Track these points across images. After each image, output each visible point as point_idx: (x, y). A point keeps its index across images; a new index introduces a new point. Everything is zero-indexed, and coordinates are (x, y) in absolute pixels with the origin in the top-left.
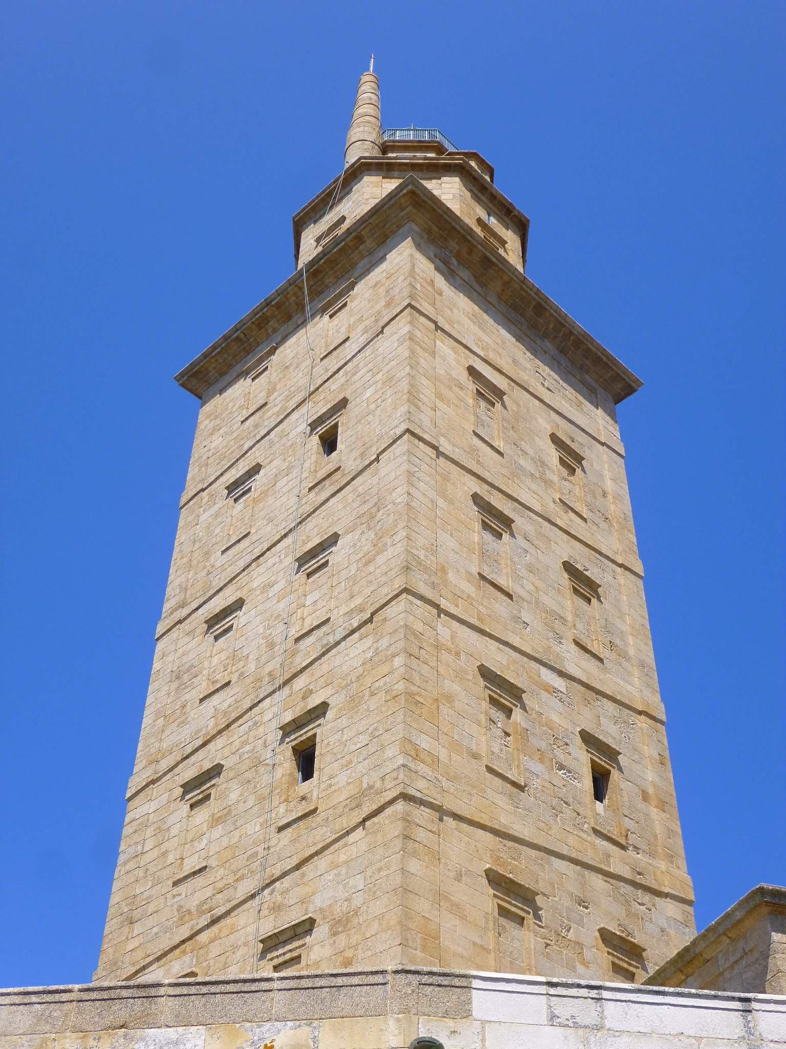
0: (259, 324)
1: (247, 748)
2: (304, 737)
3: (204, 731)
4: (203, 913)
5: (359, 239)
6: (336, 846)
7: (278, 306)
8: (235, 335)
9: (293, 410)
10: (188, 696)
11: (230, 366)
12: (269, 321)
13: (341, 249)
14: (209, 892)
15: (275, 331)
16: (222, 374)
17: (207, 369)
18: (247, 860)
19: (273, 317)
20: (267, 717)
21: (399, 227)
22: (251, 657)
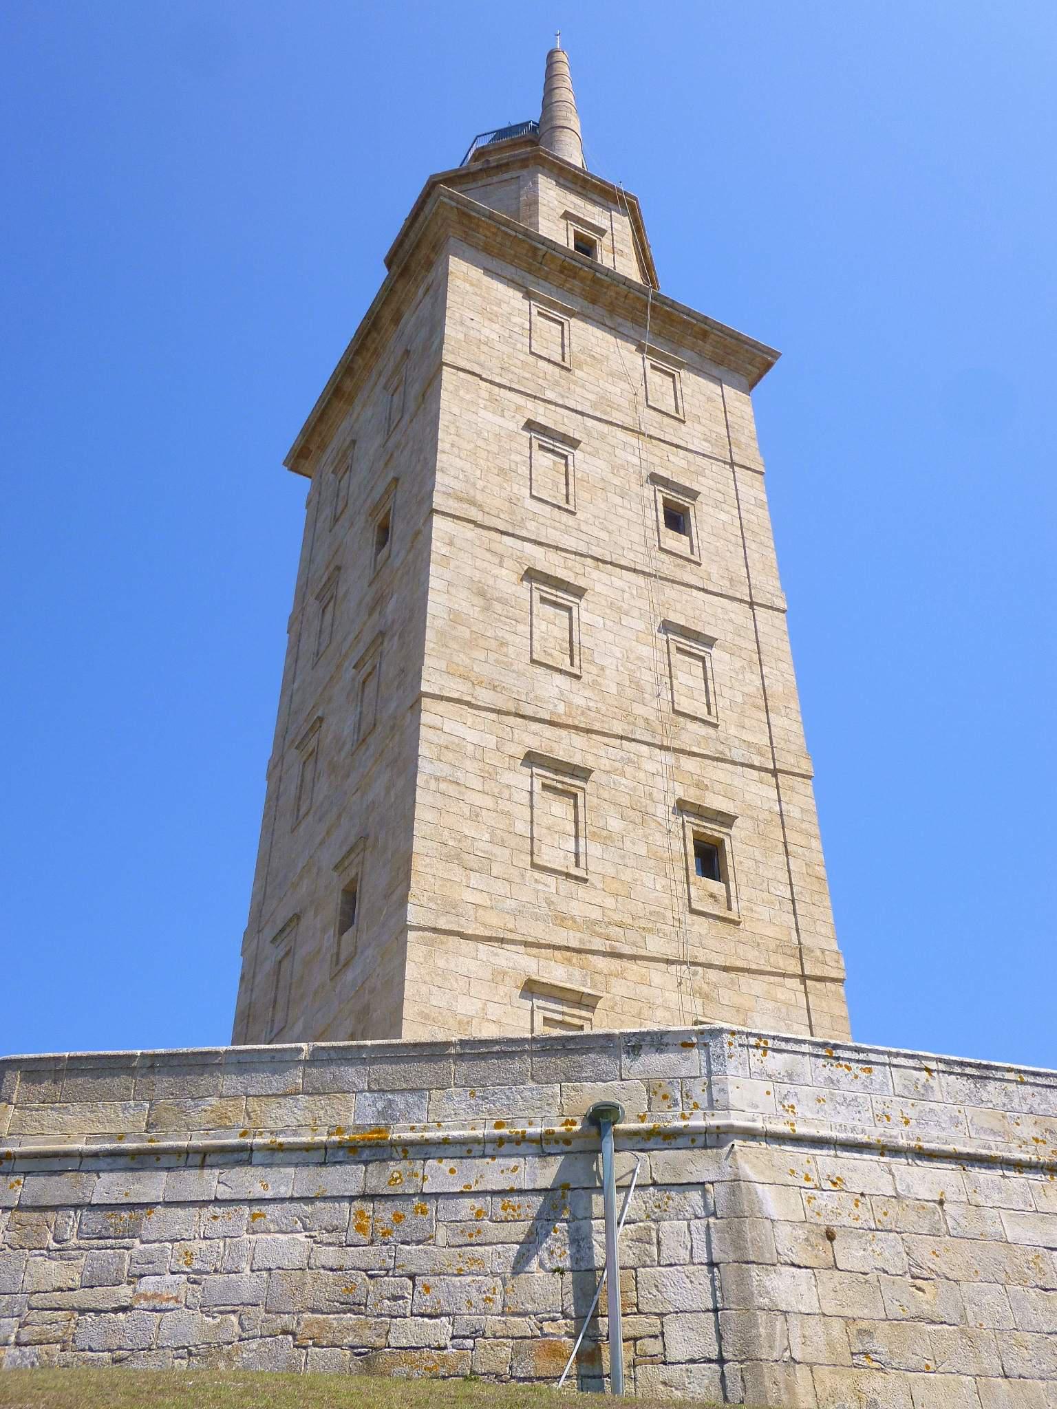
0: (565, 268)
1: (623, 781)
2: (709, 832)
3: (551, 707)
4: (599, 935)
5: (704, 335)
6: (772, 979)
7: (595, 281)
8: (540, 246)
9: (618, 425)
10: (509, 637)
11: (501, 256)
12: (574, 278)
13: (689, 323)
14: (596, 914)
15: (571, 291)
16: (487, 250)
17: (478, 226)
18: (651, 913)
19: (582, 280)
20: (650, 766)
21: (736, 370)
22: (607, 672)
